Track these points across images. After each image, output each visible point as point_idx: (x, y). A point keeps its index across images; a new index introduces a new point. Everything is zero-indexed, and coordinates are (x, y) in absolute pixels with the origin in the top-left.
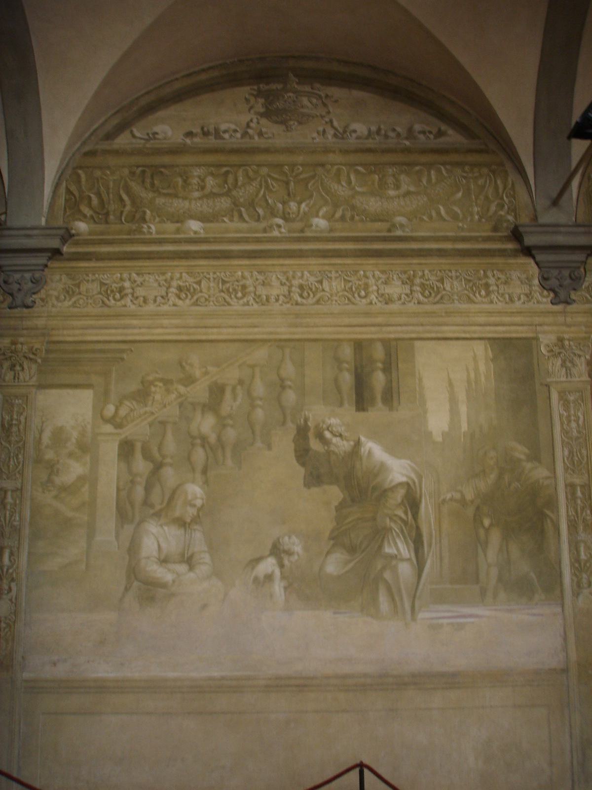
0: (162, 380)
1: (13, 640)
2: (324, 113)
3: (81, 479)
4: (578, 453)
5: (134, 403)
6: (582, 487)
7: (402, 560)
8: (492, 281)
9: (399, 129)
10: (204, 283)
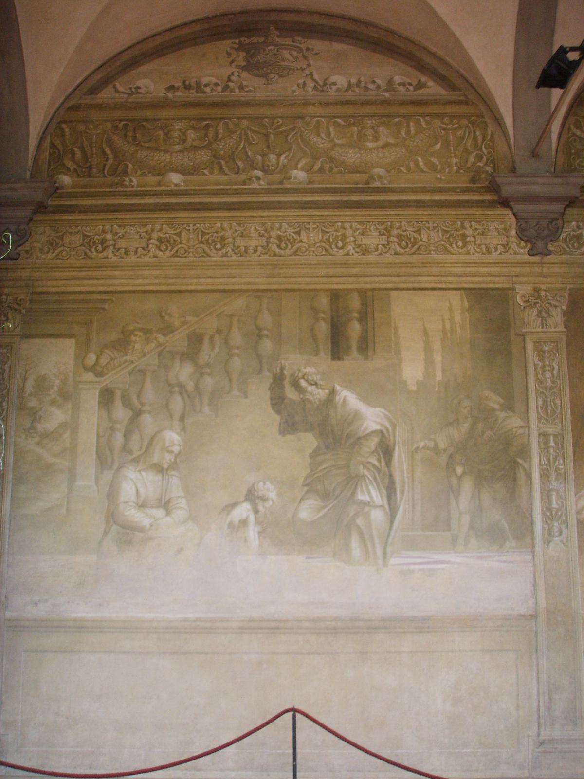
0: (141, 329)
2: (304, 67)
3: (63, 425)
4: (552, 404)
5: (115, 352)
6: (555, 436)
7: (375, 507)
8: (469, 232)
9: (379, 81)
10: (183, 234)
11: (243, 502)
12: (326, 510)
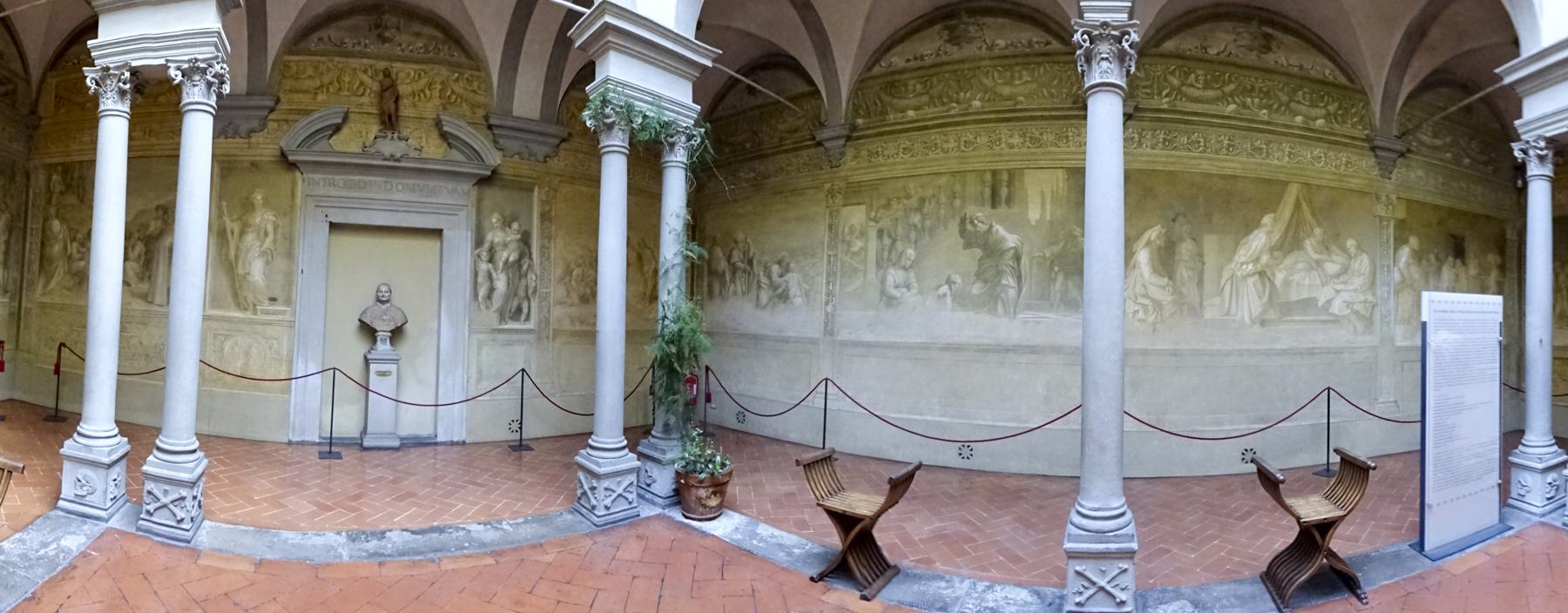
3: (861, 248)
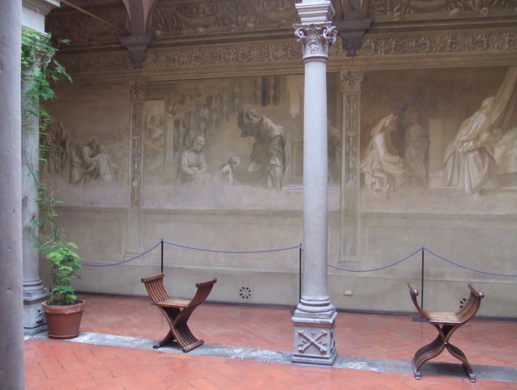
0: (189, 96)
1: (139, 195)
3: (161, 135)
6: (353, 137)
7: (277, 166)
10: (205, 55)
11: (227, 164)
12: (258, 168)
